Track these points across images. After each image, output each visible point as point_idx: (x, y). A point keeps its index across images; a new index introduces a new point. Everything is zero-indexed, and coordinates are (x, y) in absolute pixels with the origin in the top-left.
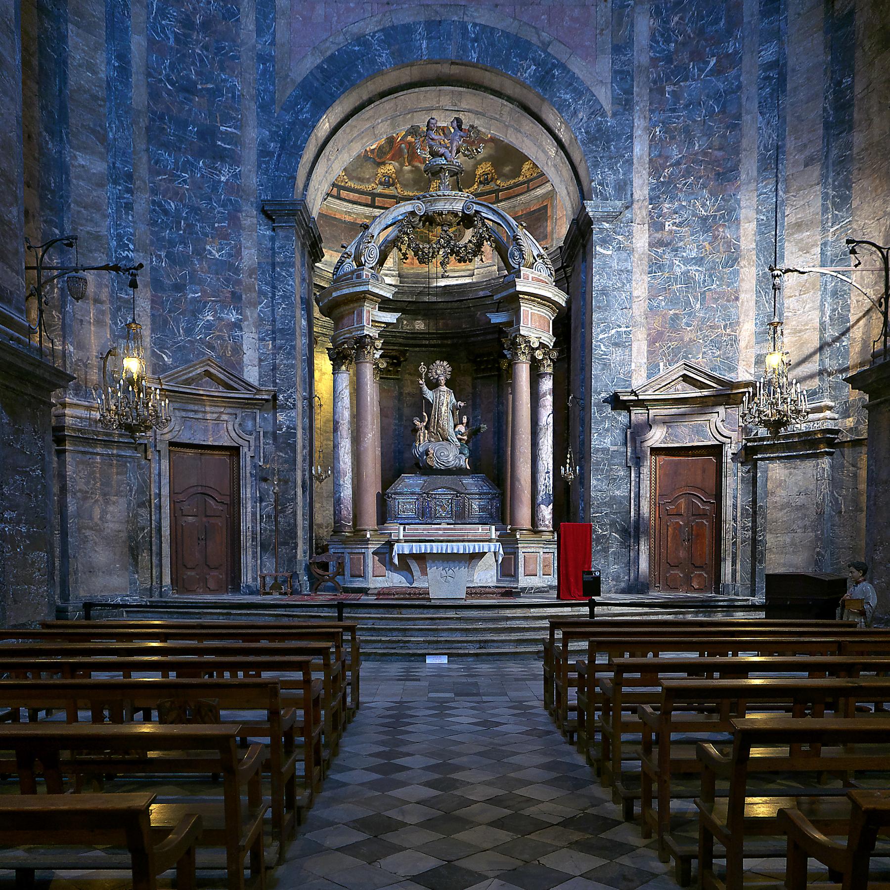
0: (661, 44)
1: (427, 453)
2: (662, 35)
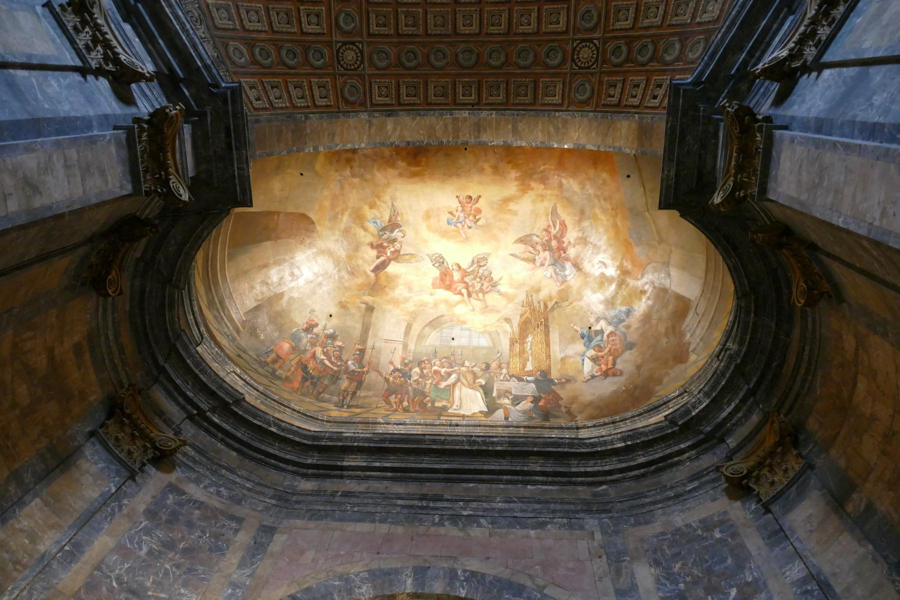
0: (668, 585)
2: (668, 579)
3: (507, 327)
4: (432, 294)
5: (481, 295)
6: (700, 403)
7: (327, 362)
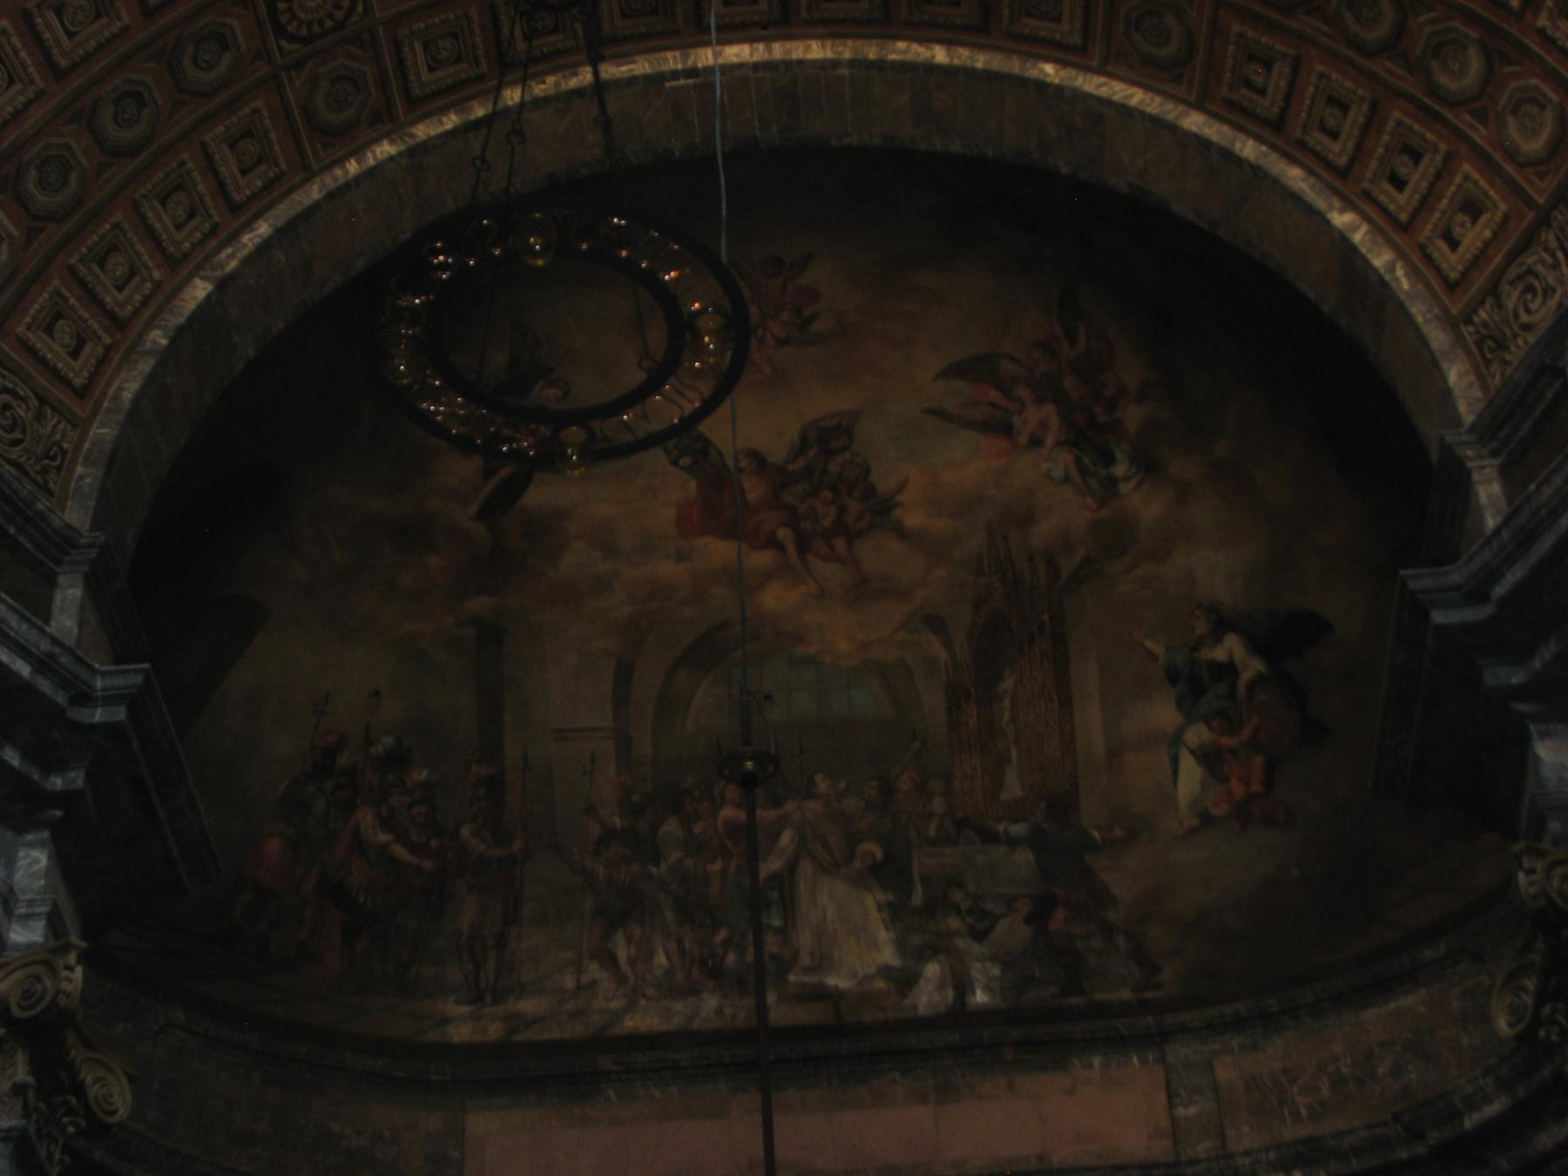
3: (934, 645)
4: (680, 557)
5: (840, 545)
6: (1487, 1100)
7: (399, 851)
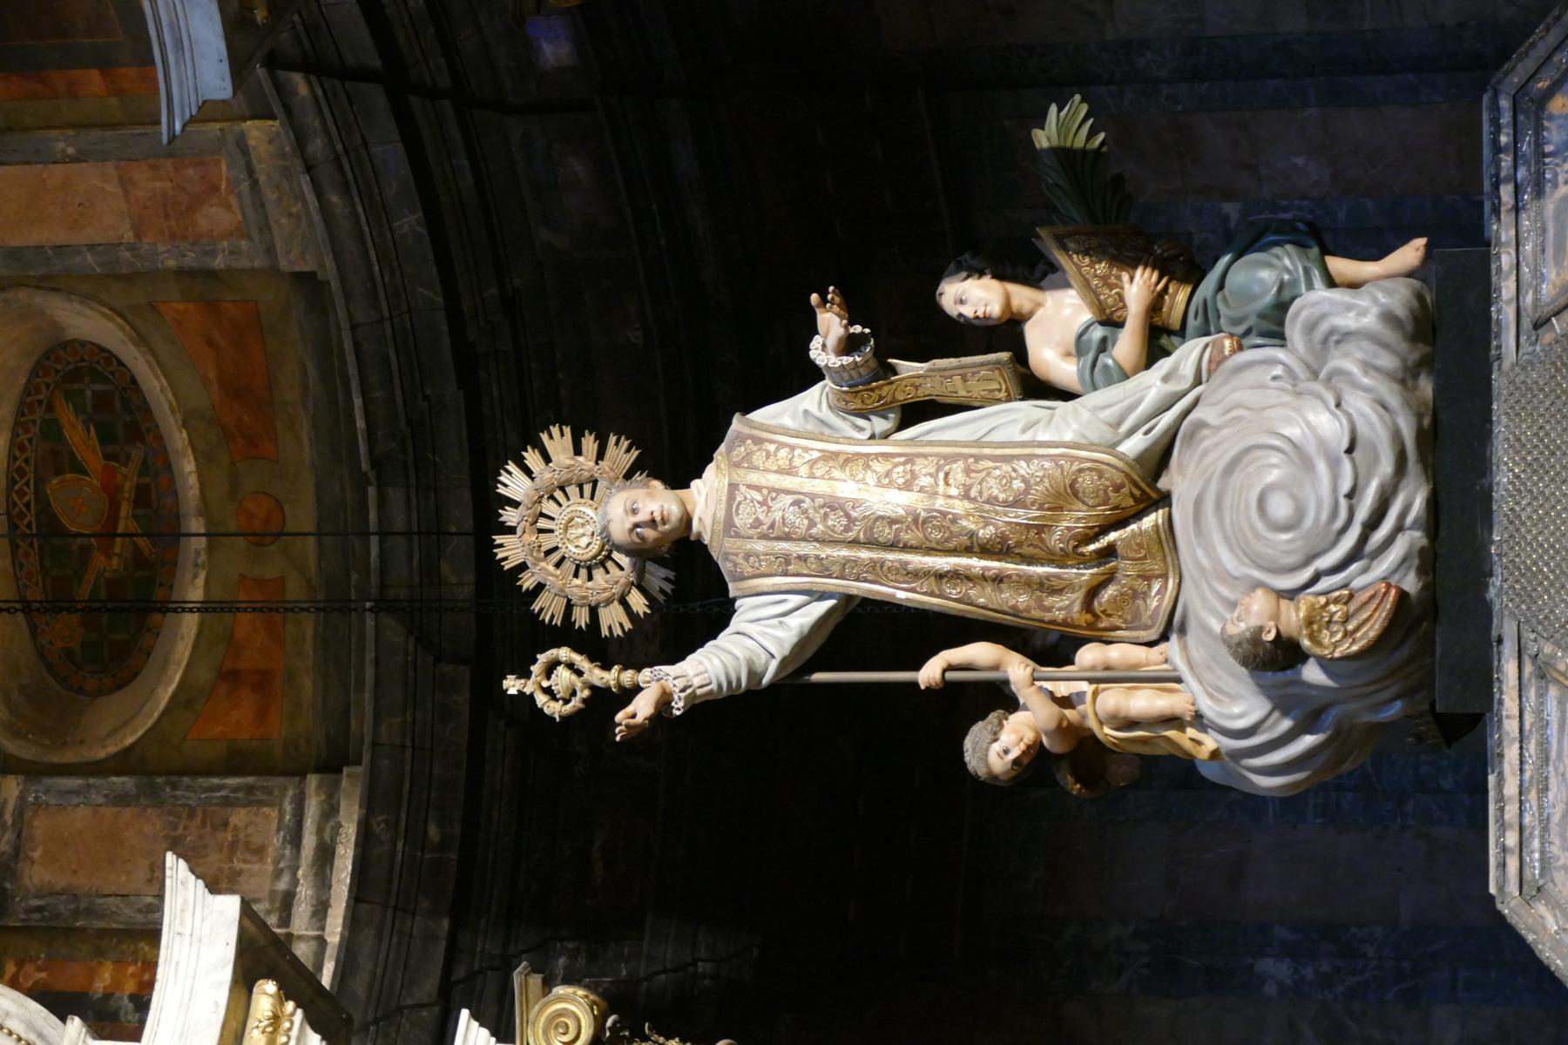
1: (1273, 658)
